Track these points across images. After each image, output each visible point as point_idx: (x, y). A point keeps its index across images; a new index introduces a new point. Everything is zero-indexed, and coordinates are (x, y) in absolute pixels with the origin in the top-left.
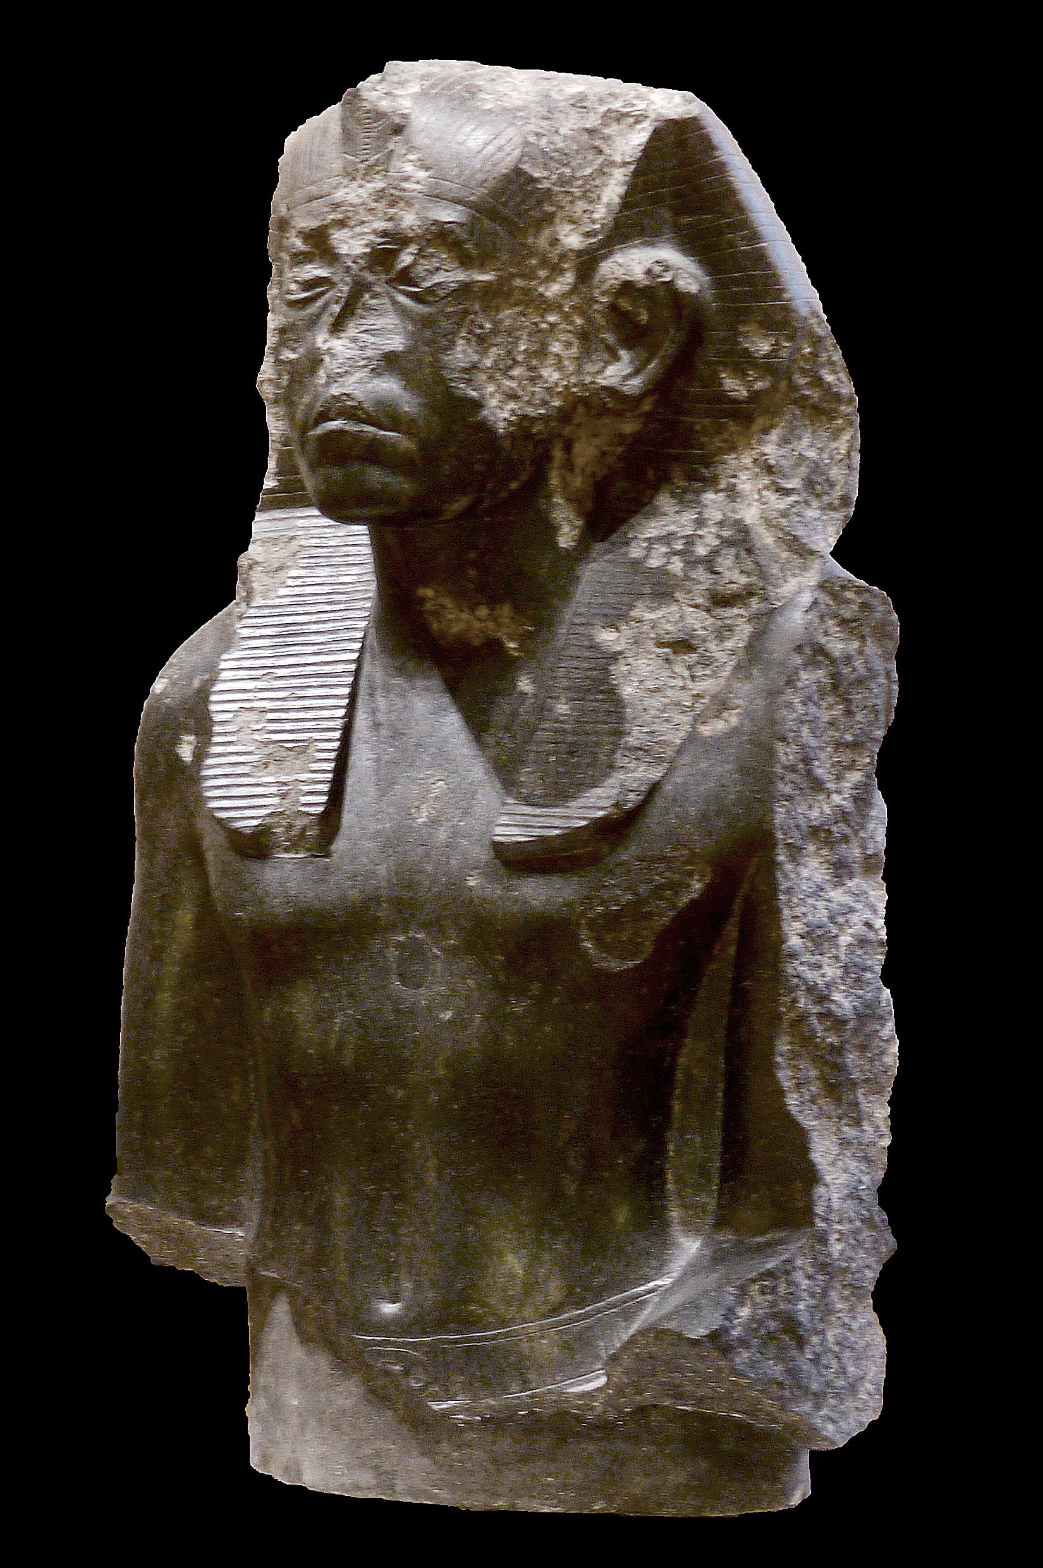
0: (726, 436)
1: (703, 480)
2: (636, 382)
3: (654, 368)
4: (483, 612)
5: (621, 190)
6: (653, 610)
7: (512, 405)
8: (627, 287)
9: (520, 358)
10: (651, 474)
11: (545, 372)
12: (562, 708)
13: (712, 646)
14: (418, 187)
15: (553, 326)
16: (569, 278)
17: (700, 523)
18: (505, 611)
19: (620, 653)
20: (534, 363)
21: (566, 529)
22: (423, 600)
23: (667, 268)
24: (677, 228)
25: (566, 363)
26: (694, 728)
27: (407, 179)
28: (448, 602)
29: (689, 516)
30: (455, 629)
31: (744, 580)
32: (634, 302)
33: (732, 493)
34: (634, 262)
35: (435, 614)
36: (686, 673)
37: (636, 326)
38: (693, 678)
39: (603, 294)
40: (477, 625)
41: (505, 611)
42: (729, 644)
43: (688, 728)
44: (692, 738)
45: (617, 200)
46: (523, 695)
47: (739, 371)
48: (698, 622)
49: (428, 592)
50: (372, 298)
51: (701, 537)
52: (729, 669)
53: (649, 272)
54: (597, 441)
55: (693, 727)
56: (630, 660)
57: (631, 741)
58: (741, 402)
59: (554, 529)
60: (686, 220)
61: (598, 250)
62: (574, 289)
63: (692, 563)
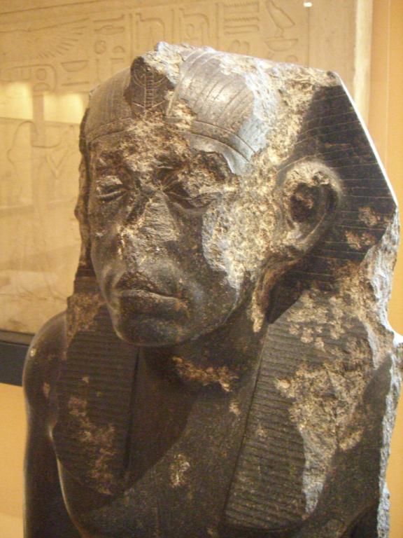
0: (346, 267)
1: (330, 290)
2: (304, 242)
3: (314, 234)
4: (211, 370)
5: (298, 128)
6: (310, 372)
7: (241, 266)
8: (302, 187)
9: (245, 236)
10: (299, 284)
11: (257, 242)
12: (261, 432)
13: (344, 395)
14: (188, 127)
15: (262, 213)
16: (273, 182)
17: (330, 317)
18: (223, 370)
19: (294, 399)
20: (253, 236)
21: (256, 320)
22: (175, 363)
23: (326, 176)
24: (323, 150)
25: (268, 234)
26: (338, 446)
27: (180, 121)
28: (191, 365)
29: (321, 311)
30: (193, 376)
31: (362, 356)
32: (305, 196)
33: (348, 300)
34: (308, 171)
35: (181, 369)
36: (332, 412)
37: (305, 209)
38: (336, 415)
39: (289, 190)
40: (206, 375)
41: (223, 370)
42: (353, 392)
43: (335, 447)
44: (338, 453)
45: (296, 134)
46: (232, 414)
47: (358, 233)
48: (338, 383)
49: (180, 360)
50: (154, 201)
51: (333, 327)
52: (353, 407)
53: (315, 178)
54: (274, 271)
55: (338, 446)
56: (301, 406)
57: (307, 464)
58: (357, 251)
59: (252, 323)
60: (328, 146)
61: (287, 164)
62: (275, 189)
63: (330, 343)
